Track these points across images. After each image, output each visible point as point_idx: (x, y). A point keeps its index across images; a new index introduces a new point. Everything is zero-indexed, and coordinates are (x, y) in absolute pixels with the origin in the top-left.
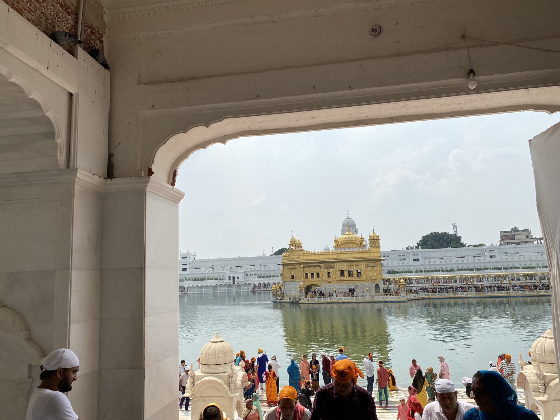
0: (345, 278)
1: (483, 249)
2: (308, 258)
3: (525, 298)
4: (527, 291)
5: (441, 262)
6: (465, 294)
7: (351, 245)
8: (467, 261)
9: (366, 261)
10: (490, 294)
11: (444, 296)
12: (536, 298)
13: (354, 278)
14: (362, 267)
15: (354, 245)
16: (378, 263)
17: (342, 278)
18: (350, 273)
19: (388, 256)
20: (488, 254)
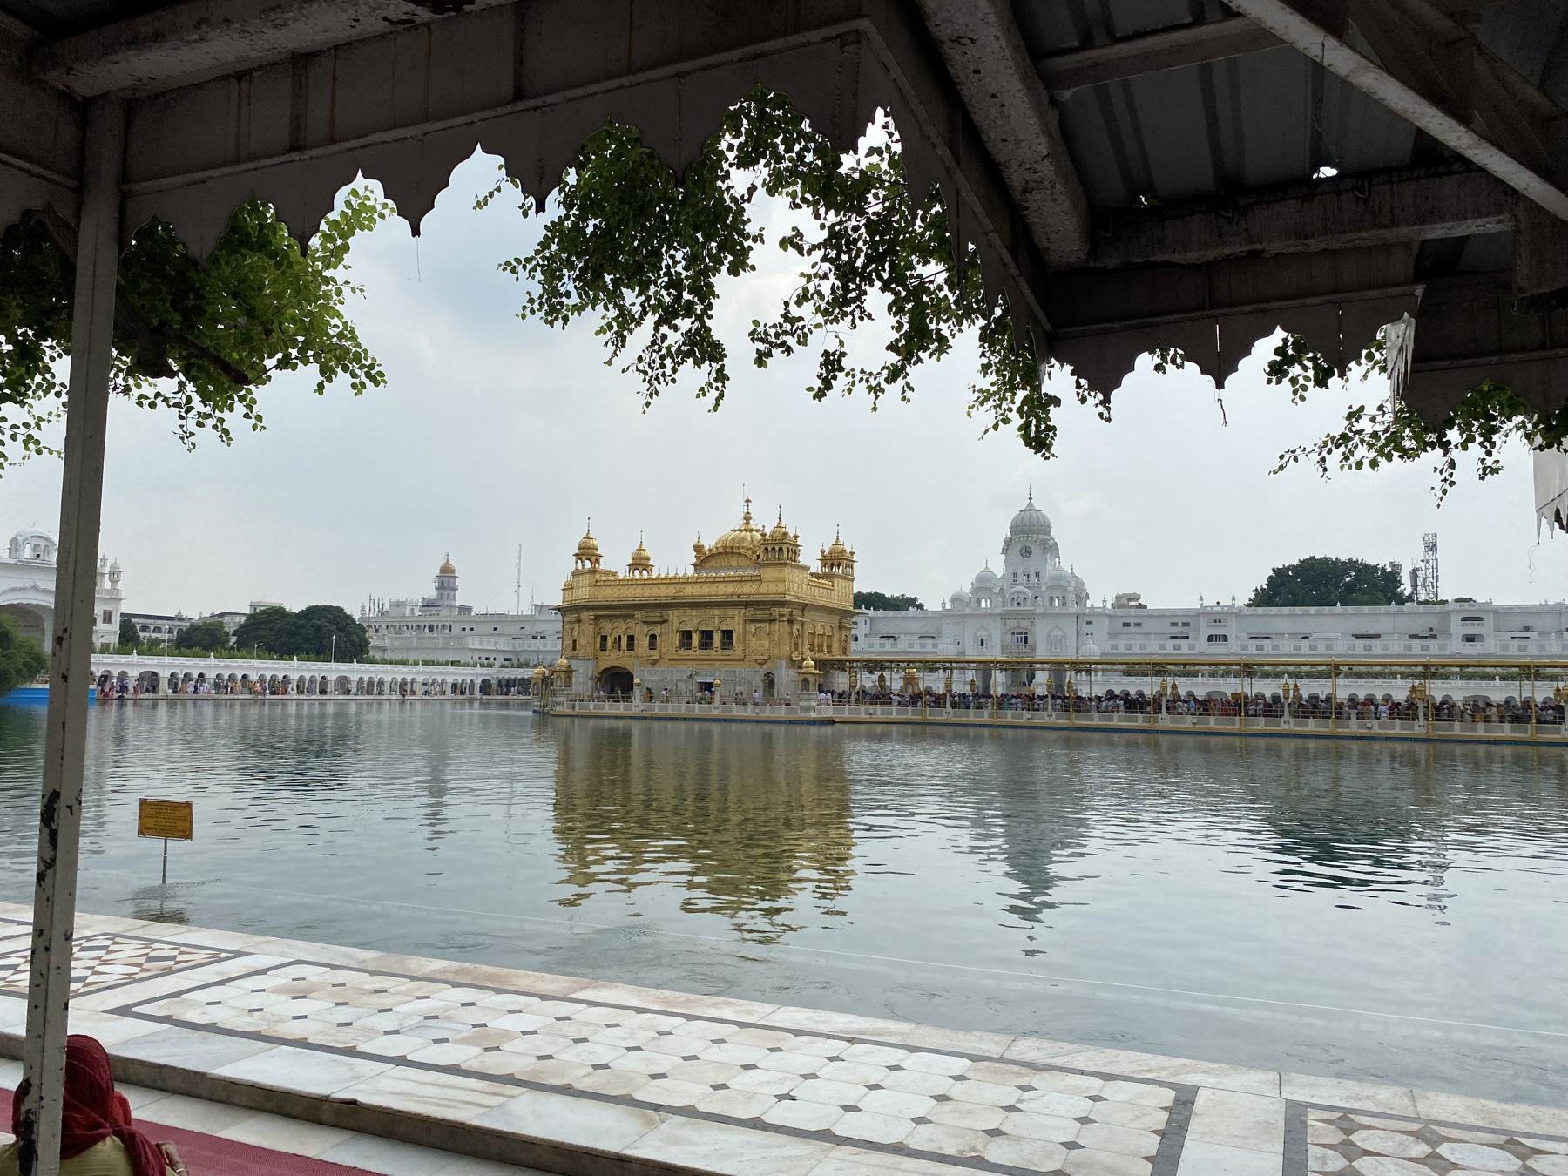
0: (691, 653)
1: (1448, 613)
2: (608, 592)
3: (1203, 738)
4: (1212, 718)
5: (1297, 648)
6: (1025, 717)
7: (734, 561)
8: (1386, 648)
9: (747, 605)
10: (1096, 720)
11: (964, 720)
12: (1237, 741)
13: (711, 653)
14: (735, 621)
15: (742, 562)
16: (776, 611)
17: (684, 653)
18: (707, 636)
19: (1138, 625)
20: (1458, 629)
